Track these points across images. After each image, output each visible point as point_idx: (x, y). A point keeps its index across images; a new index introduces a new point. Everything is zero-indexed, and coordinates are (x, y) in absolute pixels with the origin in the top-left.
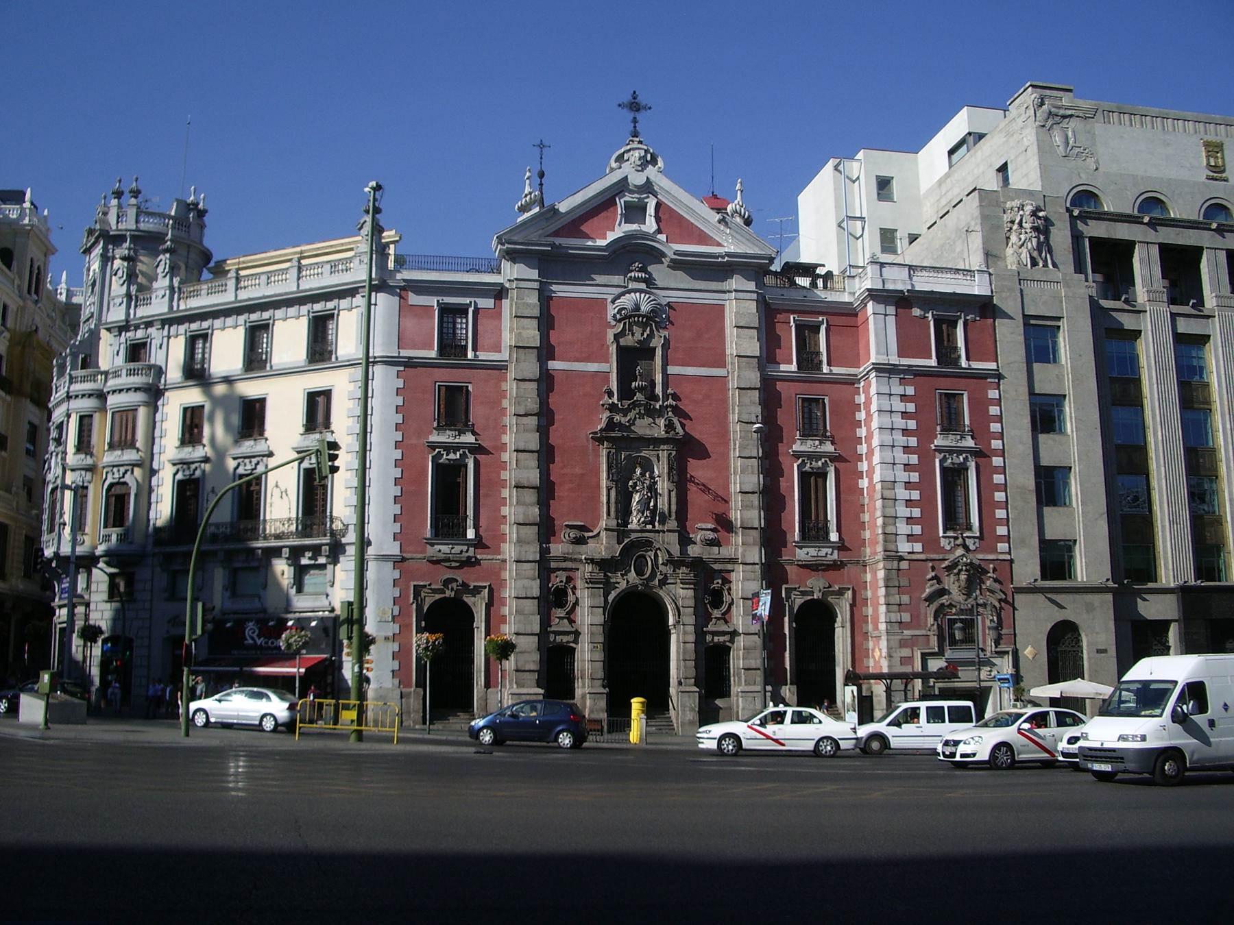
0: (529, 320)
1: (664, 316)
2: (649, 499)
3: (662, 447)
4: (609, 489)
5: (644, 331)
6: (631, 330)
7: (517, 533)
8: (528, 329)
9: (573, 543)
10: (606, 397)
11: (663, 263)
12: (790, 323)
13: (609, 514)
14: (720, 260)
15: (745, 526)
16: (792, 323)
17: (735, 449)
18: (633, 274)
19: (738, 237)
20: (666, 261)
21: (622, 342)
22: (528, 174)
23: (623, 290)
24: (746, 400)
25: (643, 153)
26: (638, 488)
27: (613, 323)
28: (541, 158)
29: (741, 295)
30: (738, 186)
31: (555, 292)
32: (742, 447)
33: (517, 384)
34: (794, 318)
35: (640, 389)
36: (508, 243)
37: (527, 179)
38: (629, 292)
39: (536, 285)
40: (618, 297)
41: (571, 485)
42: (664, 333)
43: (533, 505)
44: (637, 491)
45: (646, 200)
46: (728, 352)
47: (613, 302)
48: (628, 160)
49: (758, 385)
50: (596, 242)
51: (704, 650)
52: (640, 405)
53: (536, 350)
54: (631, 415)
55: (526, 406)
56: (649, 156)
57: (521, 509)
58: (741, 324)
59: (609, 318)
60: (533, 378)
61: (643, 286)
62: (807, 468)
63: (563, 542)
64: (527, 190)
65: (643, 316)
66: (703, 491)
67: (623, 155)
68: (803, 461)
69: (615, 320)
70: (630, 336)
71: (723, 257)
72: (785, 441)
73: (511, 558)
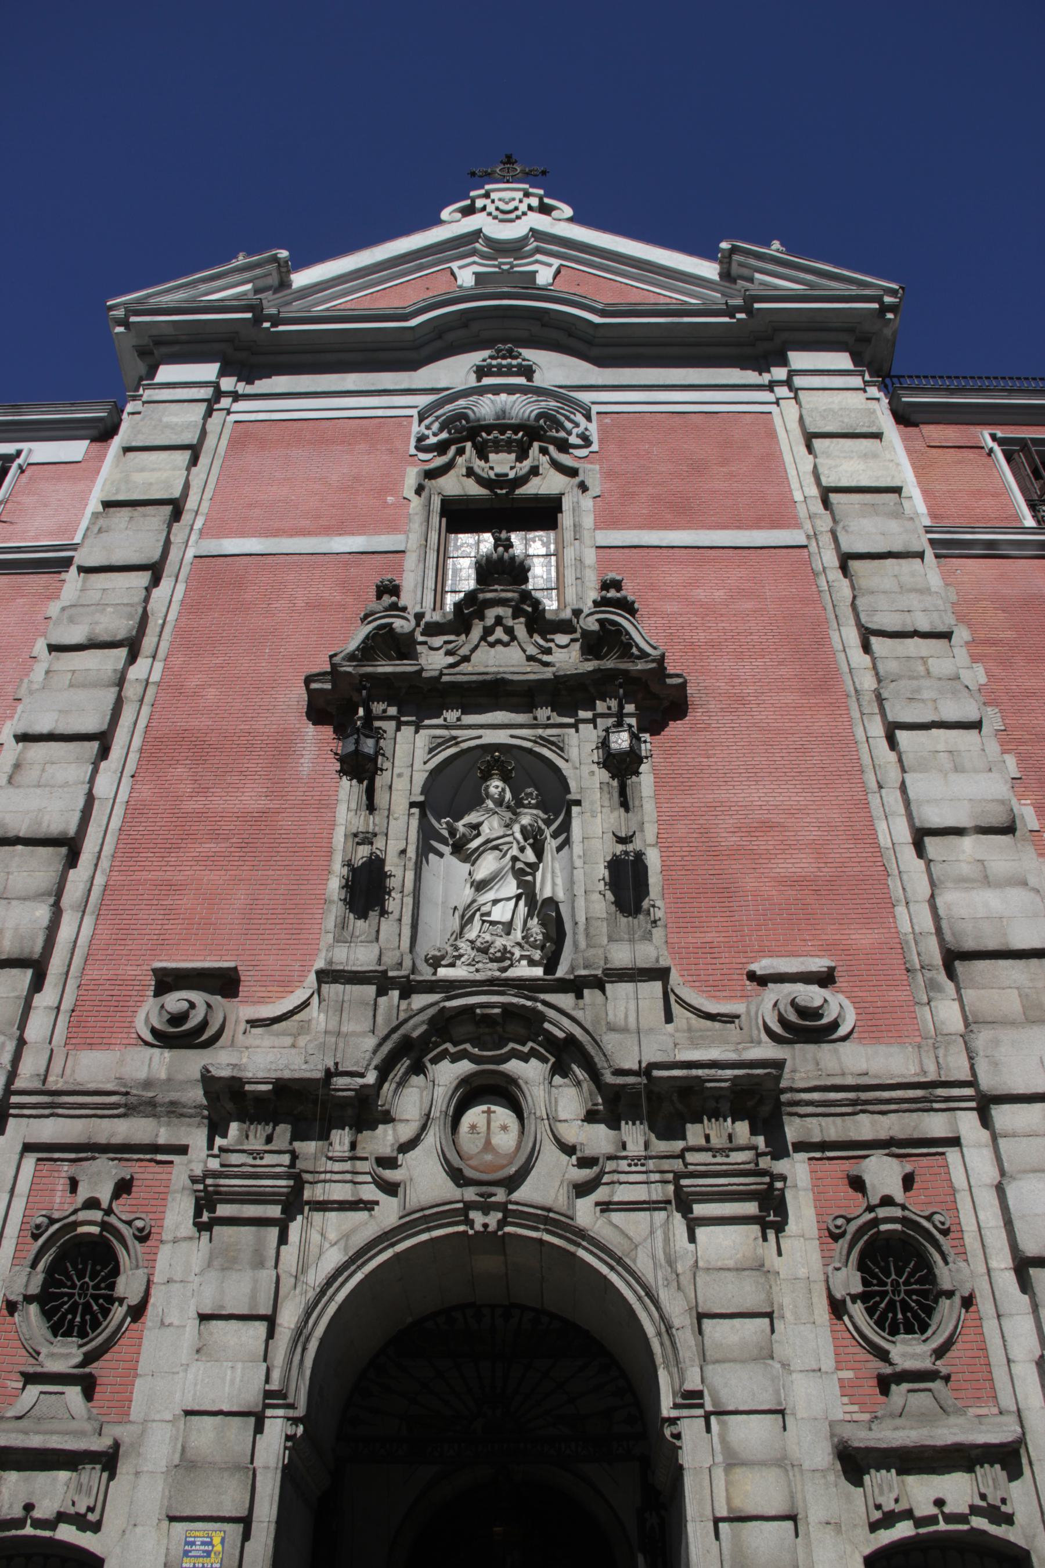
34: (994, 437)
46: (798, 496)
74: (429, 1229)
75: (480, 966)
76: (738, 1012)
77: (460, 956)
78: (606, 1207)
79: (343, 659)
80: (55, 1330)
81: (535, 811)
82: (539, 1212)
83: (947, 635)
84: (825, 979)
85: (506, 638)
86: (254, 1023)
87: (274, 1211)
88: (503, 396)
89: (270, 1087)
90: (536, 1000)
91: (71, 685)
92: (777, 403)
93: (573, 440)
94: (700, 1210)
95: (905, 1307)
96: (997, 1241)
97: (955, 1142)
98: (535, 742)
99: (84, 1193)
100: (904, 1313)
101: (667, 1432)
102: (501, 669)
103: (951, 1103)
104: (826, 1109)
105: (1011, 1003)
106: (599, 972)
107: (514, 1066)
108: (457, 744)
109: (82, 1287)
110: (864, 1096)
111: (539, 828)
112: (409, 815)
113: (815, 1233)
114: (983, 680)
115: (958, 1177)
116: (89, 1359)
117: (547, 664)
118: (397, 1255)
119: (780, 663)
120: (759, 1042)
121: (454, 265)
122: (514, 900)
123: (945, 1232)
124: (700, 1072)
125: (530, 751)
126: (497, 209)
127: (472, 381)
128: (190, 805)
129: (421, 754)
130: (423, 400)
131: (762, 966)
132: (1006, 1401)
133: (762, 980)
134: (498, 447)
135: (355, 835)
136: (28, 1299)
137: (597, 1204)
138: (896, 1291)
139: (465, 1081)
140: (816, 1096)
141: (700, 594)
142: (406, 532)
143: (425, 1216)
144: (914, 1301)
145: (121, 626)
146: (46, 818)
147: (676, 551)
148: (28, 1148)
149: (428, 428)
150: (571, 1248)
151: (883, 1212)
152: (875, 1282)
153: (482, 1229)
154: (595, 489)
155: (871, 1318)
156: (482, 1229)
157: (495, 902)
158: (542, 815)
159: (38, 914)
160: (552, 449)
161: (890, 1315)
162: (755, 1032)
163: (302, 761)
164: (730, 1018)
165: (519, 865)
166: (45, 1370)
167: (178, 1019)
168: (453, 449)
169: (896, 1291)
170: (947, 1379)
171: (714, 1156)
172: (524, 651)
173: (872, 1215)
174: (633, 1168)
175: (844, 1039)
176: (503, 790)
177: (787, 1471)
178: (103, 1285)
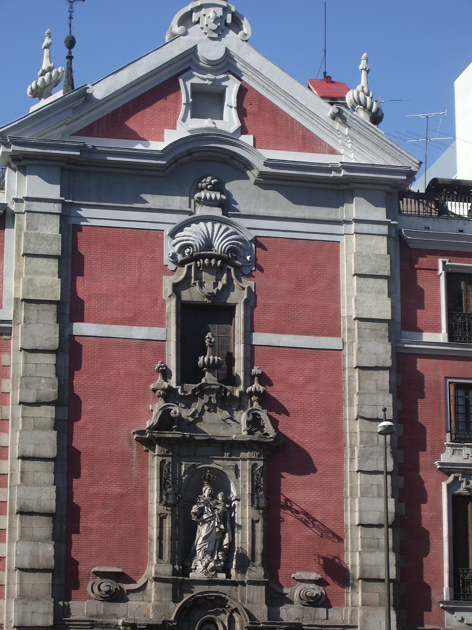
0: (45, 260)
1: (248, 258)
2: (222, 534)
3: (243, 455)
4: (161, 518)
5: (218, 279)
6: (198, 278)
7: (21, 583)
8: (42, 273)
9: (105, 599)
10: (160, 377)
11: (247, 178)
12: (437, 270)
13: (160, 555)
14: (333, 174)
15: (367, 576)
16: (441, 270)
17: (352, 459)
18: (202, 194)
19: (361, 139)
20: (252, 175)
21: (186, 295)
22: (47, 41)
23: (187, 217)
24: (370, 386)
25: (220, 12)
26: (205, 517)
27: (172, 267)
28: (71, 18)
29: (365, 228)
30: (363, 64)
31: (85, 219)
32: (363, 457)
33: (25, 357)
34: (444, 263)
35: (212, 367)
36: (14, 144)
37: (47, 47)
38: (197, 220)
39: (57, 208)
40: (180, 228)
41: (106, 511)
42: (248, 283)
43: (44, 540)
44: (204, 522)
45: (224, 84)
46: (344, 312)
47: (172, 235)
48: (198, 22)
49: (389, 363)
50: (148, 145)
52: (211, 391)
53: (54, 307)
54: (197, 406)
55: (38, 389)
56: (229, 17)
57: (27, 547)
58: (365, 271)
59: (167, 260)
60: (47, 345)
61: (217, 212)
62: (462, 489)
63: (90, 598)
64: (46, 64)
65: (217, 258)
66: (305, 523)
67: (188, 15)
68: (456, 478)
69: (175, 262)
70: (197, 288)
71: (338, 170)
72: (429, 448)
73: (9, 621)
146: (43, 503)
163: (133, 468)
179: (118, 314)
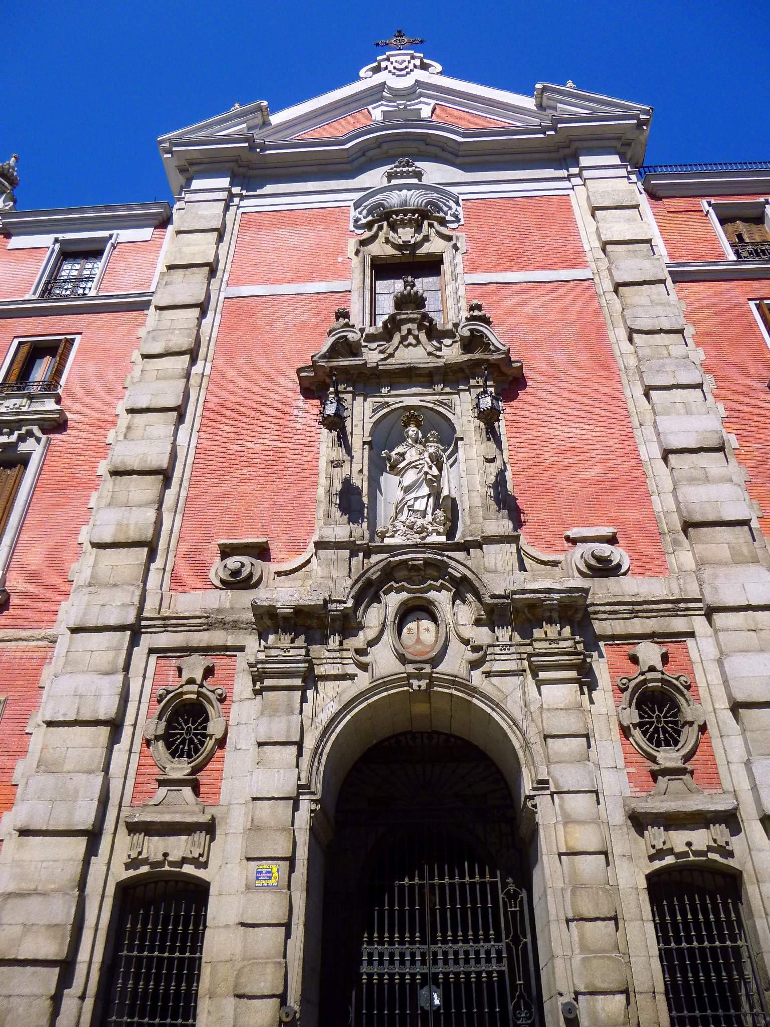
34: (710, 204)
46: (587, 247)
51: (643, 884)
74: (386, 690)
75: (409, 536)
76: (561, 560)
77: (397, 531)
78: (488, 674)
79: (319, 358)
80: (173, 755)
81: (436, 445)
82: (450, 678)
83: (680, 331)
84: (612, 540)
85: (414, 342)
86: (278, 574)
87: (298, 682)
88: (405, 192)
89: (292, 610)
90: (443, 555)
91: (157, 379)
92: (573, 189)
93: (449, 218)
94: (542, 675)
95: (665, 731)
96: (720, 693)
97: (692, 635)
98: (435, 404)
99: (186, 676)
100: (664, 735)
101: (529, 804)
102: (413, 361)
103: (689, 613)
104: (614, 616)
105: (724, 553)
106: (479, 538)
107: (432, 595)
108: (389, 406)
109: (187, 729)
110: (637, 608)
111: (440, 455)
112: (363, 449)
113: (610, 688)
114: (703, 357)
115: (694, 655)
116: (195, 771)
117: (439, 357)
118: (369, 704)
119: (579, 352)
120: (573, 577)
121: (370, 108)
122: (427, 497)
123: (688, 687)
124: (540, 595)
125: (432, 409)
126: (395, 68)
127: (385, 183)
128: (234, 448)
129: (368, 413)
130: (357, 196)
131: (573, 533)
132: (727, 785)
133: (574, 541)
134: (404, 224)
135: (332, 462)
136: (157, 738)
137: (483, 673)
138: (659, 721)
139: (404, 603)
140: (608, 608)
141: (529, 311)
142: (351, 279)
143: (384, 682)
144: (669, 727)
145: (186, 342)
146: (149, 458)
147: (514, 285)
148: (151, 651)
149: (360, 213)
150: (469, 698)
151: (649, 676)
152: (646, 716)
153: (418, 688)
154: (463, 249)
155: (645, 737)
156: (418, 688)
157: (416, 499)
158: (440, 446)
159: (148, 515)
160: (435, 224)
161: (656, 735)
162: (571, 571)
164: (555, 564)
165: (429, 477)
166: (170, 777)
167: (235, 573)
168: (376, 226)
169: (659, 721)
170: (692, 773)
171: (550, 644)
172: (426, 349)
173: (643, 677)
174: (503, 652)
175: (625, 574)
176: (417, 433)
177: (599, 825)
178: (199, 728)
179: (290, 275)
